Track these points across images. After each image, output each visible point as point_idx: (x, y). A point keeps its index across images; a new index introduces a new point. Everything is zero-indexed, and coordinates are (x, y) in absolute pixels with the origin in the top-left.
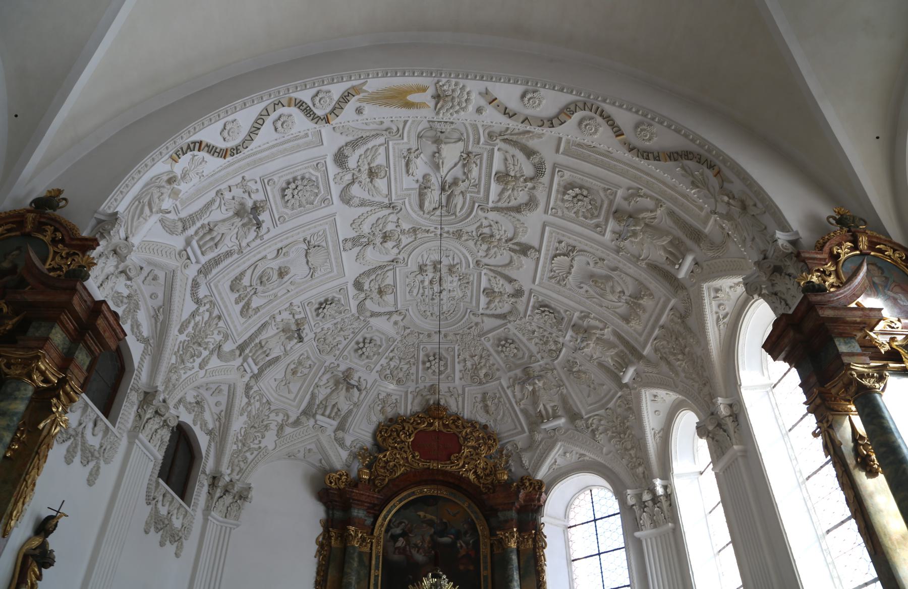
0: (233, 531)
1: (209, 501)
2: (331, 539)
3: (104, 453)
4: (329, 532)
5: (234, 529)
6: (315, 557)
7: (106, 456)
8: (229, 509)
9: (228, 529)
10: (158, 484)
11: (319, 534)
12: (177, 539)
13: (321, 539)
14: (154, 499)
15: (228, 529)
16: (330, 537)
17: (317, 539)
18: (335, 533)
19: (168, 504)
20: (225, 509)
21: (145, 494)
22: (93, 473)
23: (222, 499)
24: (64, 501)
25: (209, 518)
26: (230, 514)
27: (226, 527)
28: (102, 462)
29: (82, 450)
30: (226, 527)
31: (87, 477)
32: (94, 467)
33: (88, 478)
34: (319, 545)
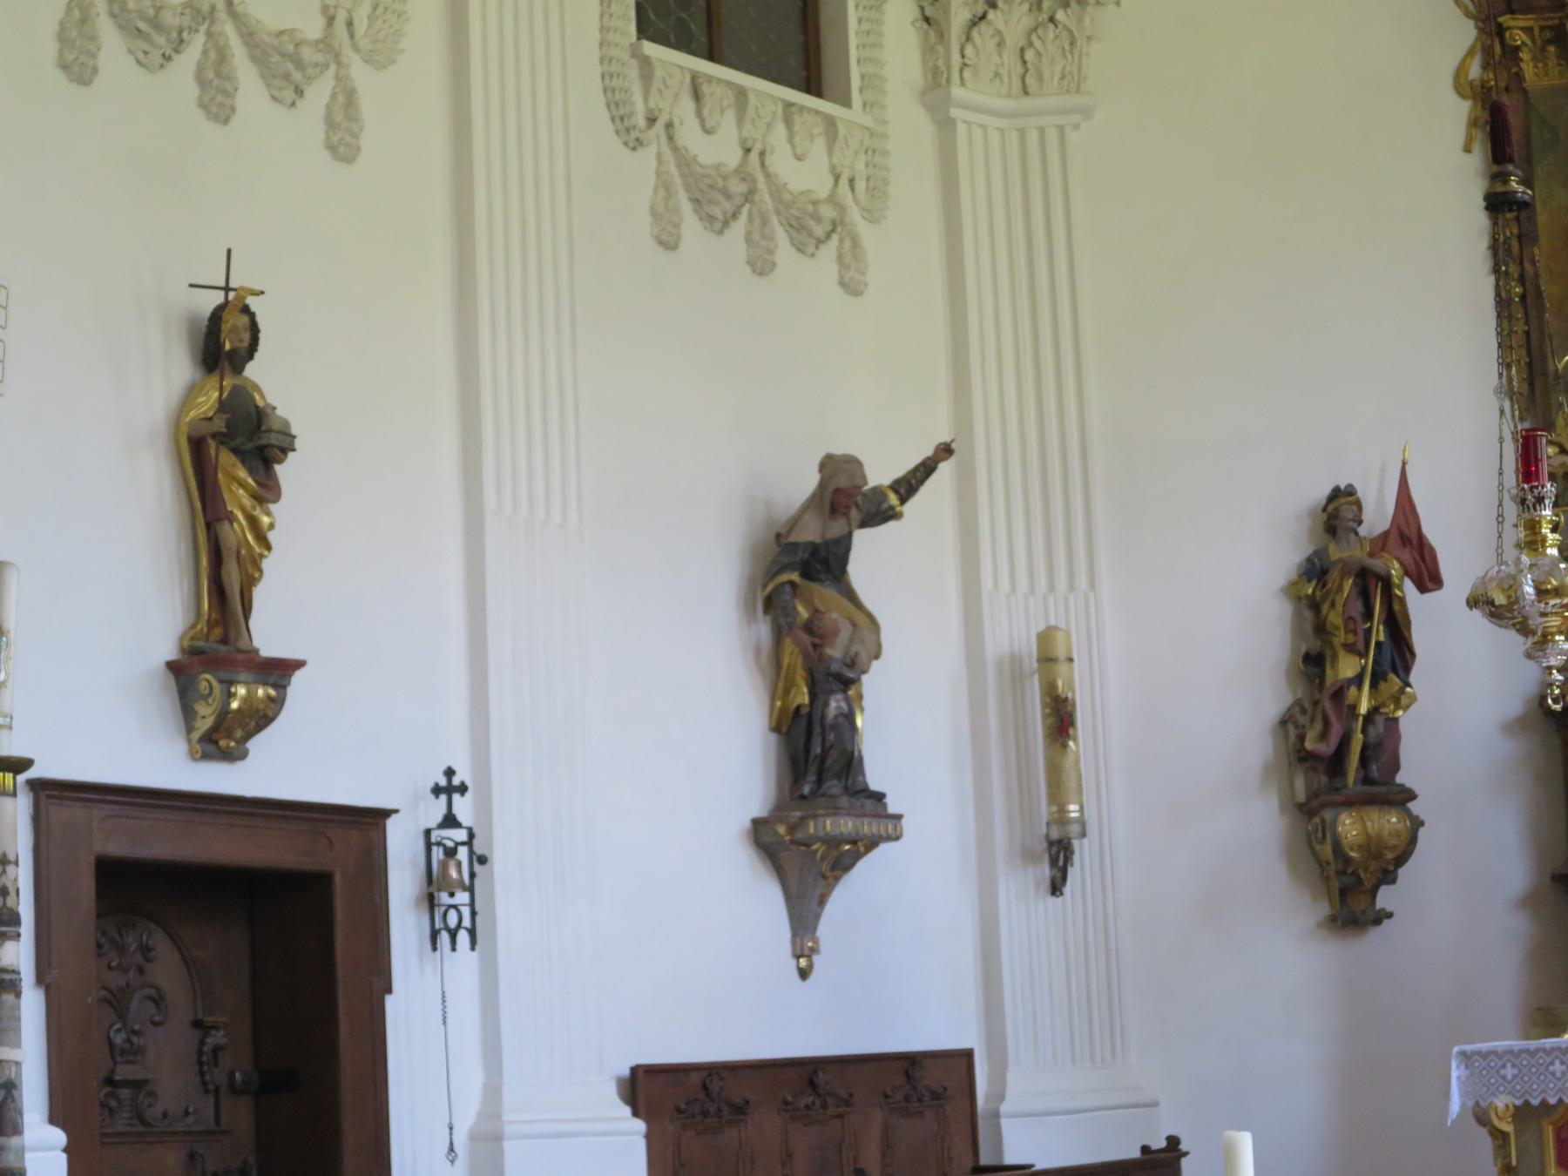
0: (1073, 137)
1: (932, 49)
2: (1517, 60)
3: (352, 36)
4: (1500, 31)
5: (1077, 127)
6: (1467, 150)
7: (364, 44)
8: (1029, 55)
9: (1052, 138)
10: (646, 64)
11: (1460, 53)
12: (819, 231)
13: (1475, 71)
14: (652, 121)
15: (1052, 138)
16: (1512, 53)
17: (1460, 74)
18: (1528, 30)
19: (730, 116)
20: (1010, 59)
21: (606, 116)
22: (339, 117)
23: (983, 26)
24: (229, 252)
25: (955, 112)
26: (1040, 78)
27: (1042, 130)
28: (359, 71)
29: (254, 59)
30: (1042, 130)
31: (322, 136)
32: (334, 96)
33: (328, 138)
34: (1474, 98)
